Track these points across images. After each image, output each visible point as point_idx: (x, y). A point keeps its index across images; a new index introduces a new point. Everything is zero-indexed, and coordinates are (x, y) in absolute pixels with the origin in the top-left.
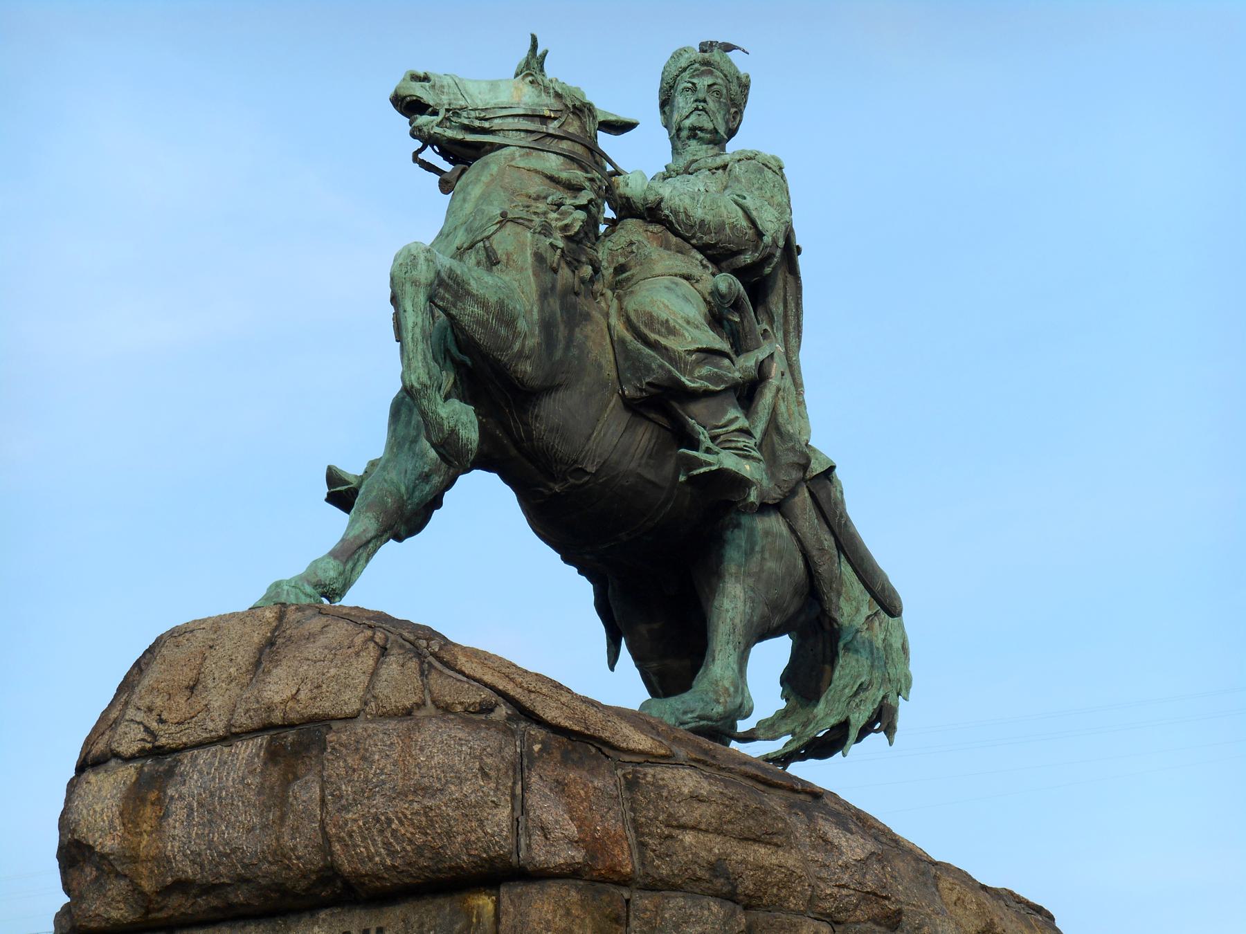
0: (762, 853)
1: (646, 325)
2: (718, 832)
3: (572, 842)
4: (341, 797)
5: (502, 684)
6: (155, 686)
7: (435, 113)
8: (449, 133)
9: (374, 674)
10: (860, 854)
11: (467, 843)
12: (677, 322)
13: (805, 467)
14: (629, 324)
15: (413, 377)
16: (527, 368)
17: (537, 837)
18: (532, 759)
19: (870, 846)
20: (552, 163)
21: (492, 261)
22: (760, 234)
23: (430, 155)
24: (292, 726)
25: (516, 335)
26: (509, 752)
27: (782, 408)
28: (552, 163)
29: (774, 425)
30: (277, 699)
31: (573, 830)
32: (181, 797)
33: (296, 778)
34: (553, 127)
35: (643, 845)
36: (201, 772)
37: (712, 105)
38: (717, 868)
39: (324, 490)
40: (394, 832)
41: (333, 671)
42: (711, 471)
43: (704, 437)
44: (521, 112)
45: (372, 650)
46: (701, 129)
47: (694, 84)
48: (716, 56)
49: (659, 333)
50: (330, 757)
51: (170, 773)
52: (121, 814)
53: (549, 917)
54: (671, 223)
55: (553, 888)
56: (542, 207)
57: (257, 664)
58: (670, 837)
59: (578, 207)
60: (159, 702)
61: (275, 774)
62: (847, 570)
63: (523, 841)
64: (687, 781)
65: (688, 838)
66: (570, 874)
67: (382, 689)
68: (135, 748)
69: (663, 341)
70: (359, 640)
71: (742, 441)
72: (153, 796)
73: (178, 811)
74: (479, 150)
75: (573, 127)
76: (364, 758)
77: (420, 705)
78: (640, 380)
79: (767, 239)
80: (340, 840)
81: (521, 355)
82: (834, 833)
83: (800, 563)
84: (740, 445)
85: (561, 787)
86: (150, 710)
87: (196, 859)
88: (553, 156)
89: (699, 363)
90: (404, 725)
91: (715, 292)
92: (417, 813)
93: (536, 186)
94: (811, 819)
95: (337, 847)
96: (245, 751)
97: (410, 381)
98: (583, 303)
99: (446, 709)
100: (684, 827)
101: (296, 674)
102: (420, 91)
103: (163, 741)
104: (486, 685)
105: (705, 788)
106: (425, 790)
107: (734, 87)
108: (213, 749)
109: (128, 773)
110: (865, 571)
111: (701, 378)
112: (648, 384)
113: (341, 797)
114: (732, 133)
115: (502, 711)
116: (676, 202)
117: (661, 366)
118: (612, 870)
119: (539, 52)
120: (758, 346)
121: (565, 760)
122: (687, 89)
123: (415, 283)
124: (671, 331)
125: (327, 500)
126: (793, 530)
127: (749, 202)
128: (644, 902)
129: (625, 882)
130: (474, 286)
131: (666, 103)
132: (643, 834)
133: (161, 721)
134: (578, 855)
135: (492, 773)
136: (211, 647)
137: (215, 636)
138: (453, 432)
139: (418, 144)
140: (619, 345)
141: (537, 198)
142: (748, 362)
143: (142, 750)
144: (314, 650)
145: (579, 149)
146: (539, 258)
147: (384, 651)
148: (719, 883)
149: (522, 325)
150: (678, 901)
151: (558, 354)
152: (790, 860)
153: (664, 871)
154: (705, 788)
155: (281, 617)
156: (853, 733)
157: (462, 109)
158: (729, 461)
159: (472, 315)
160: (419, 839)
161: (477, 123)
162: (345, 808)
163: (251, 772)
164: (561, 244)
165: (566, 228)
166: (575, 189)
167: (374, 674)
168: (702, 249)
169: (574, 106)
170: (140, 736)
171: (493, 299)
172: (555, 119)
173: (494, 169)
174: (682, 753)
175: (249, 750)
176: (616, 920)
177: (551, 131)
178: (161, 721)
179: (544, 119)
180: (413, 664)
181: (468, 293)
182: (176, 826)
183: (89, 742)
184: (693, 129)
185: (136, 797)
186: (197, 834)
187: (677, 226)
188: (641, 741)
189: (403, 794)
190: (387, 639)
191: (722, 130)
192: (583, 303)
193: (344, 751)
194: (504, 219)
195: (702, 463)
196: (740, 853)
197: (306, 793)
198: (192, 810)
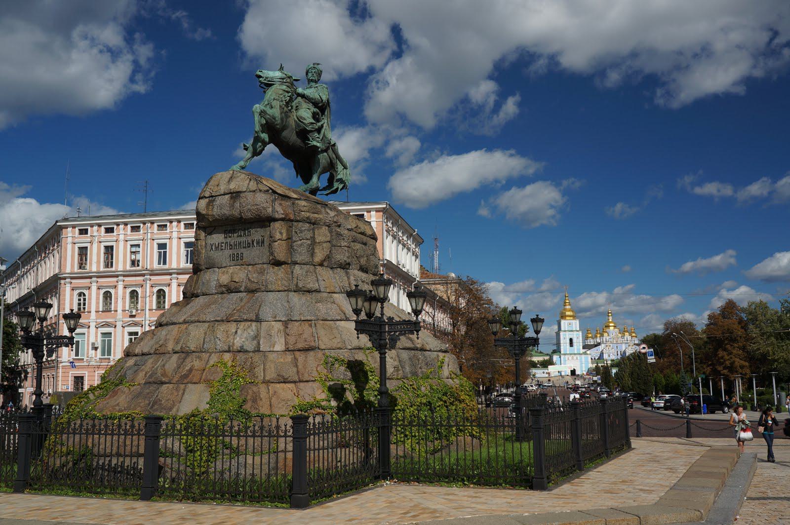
0: (316, 215)
3: (283, 214)
8: (266, 82)
9: (249, 184)
10: (333, 215)
12: (306, 118)
13: (330, 143)
14: (297, 117)
16: (278, 126)
17: (276, 213)
18: (276, 199)
19: (336, 213)
20: (284, 87)
21: (272, 107)
22: (322, 100)
24: (234, 193)
25: (276, 121)
26: (271, 198)
27: (326, 133)
28: (284, 87)
29: (324, 135)
31: (282, 212)
34: (285, 81)
35: (295, 214)
37: (315, 75)
38: (308, 218)
43: (311, 139)
45: (249, 180)
48: (316, 66)
51: (214, 200)
56: (282, 96)
57: (229, 181)
59: (288, 96)
60: (212, 188)
61: (232, 201)
62: (338, 162)
64: (303, 203)
65: (303, 213)
66: (282, 219)
67: (250, 187)
70: (246, 178)
71: (318, 139)
72: (211, 204)
74: (270, 85)
75: (289, 80)
79: (324, 101)
81: (277, 125)
82: (329, 211)
83: (329, 160)
85: (281, 204)
87: (219, 215)
89: (310, 125)
91: (314, 112)
93: (281, 92)
94: (325, 209)
95: (242, 214)
98: (289, 114)
99: (261, 191)
100: (301, 211)
102: (260, 73)
105: (306, 204)
106: (257, 205)
107: (319, 72)
109: (207, 200)
114: (319, 80)
115: (271, 191)
116: (307, 94)
120: (321, 121)
121: (282, 200)
123: (257, 112)
124: (305, 119)
126: (328, 154)
128: (295, 224)
129: (292, 221)
130: (268, 112)
131: (307, 74)
134: (283, 216)
138: (264, 139)
139: (260, 84)
140: (295, 121)
141: (281, 94)
142: (319, 124)
144: (238, 179)
145: (289, 85)
146: (280, 106)
147: (250, 180)
148: (308, 221)
149: (277, 119)
150: (301, 223)
151: (284, 124)
152: (321, 216)
153: (299, 219)
154: (306, 204)
155: (233, 173)
156: (339, 190)
158: (315, 143)
160: (256, 213)
162: (244, 207)
164: (285, 103)
165: (286, 100)
166: (288, 92)
167: (249, 184)
168: (312, 103)
171: (271, 115)
173: (273, 89)
174: (302, 198)
176: (290, 227)
179: (283, 79)
180: (255, 182)
182: (215, 210)
183: (201, 194)
184: (312, 80)
185: (208, 205)
188: (295, 196)
189: (253, 205)
191: (317, 80)
192: (289, 114)
194: (274, 99)
196: (312, 215)
197: (237, 205)
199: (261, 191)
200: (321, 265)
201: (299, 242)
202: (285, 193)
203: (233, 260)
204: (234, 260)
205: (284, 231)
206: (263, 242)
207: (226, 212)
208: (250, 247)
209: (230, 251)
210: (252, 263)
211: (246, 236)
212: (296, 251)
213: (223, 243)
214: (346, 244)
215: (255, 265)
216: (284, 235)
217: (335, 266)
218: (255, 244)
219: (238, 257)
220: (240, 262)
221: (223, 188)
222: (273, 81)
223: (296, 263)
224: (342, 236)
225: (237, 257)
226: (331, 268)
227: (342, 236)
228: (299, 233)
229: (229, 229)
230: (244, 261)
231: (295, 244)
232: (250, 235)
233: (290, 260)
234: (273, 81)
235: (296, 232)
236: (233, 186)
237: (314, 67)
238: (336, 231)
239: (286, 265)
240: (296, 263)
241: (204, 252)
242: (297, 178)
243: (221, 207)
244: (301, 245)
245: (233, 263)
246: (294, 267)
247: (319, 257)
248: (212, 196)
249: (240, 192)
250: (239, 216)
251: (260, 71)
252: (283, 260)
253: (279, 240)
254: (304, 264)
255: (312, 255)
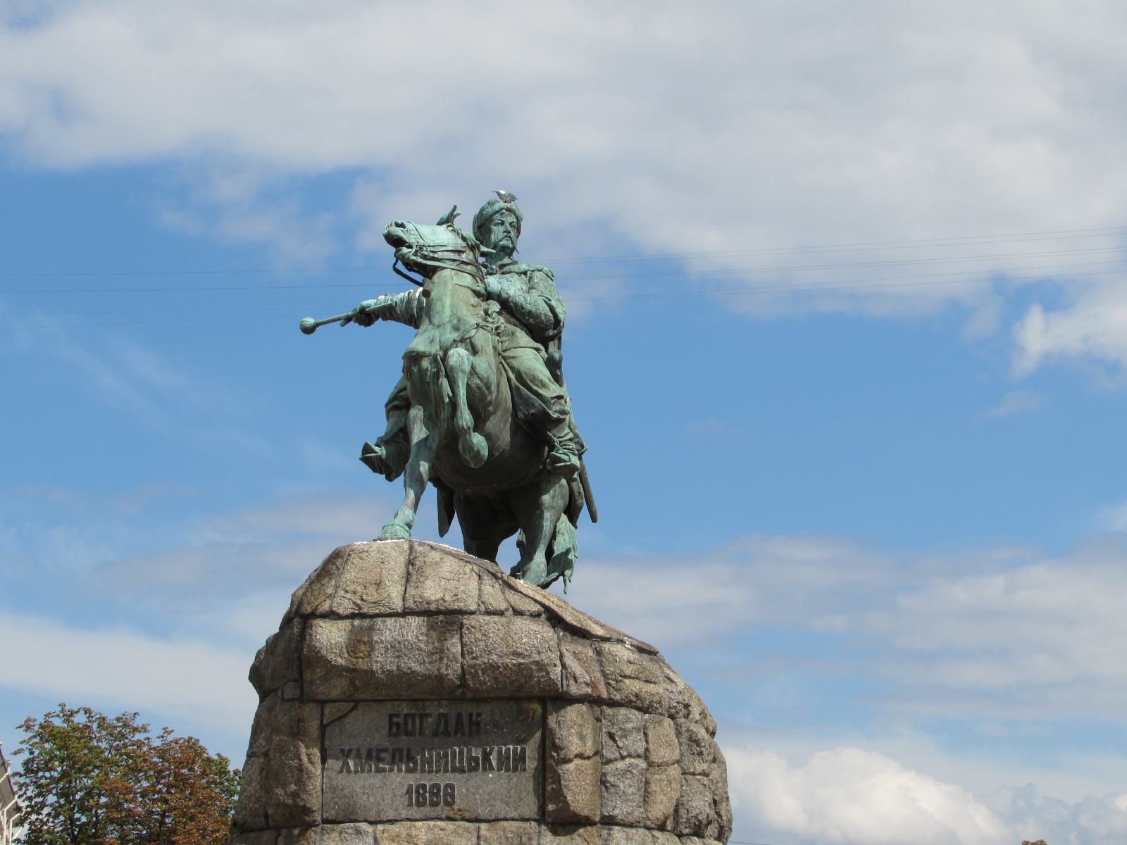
1: (531, 381)
2: (637, 678)
3: (587, 684)
4: (472, 653)
5: (547, 603)
6: (355, 580)
7: (410, 247)
9: (480, 590)
11: (539, 682)
15: (464, 424)
17: (572, 682)
23: (400, 266)
24: (438, 612)
25: (490, 393)
30: (433, 598)
32: (382, 642)
33: (446, 640)
35: (609, 684)
36: (390, 630)
39: (359, 454)
40: (501, 673)
41: (462, 588)
42: (566, 465)
44: (450, 249)
46: (508, 248)
47: (503, 221)
49: (537, 386)
50: (467, 632)
51: (371, 628)
52: (347, 647)
53: (575, 719)
54: (512, 310)
55: (576, 706)
58: (621, 681)
63: (564, 682)
65: (627, 681)
68: (348, 612)
69: (541, 391)
73: (380, 648)
76: (484, 635)
77: (507, 610)
78: (528, 411)
80: (471, 673)
84: (570, 447)
86: (354, 593)
88: (468, 275)
90: (503, 619)
92: (514, 665)
96: (415, 622)
97: (463, 425)
99: (518, 613)
100: (625, 677)
101: (439, 586)
102: (399, 232)
103: (365, 610)
104: (536, 601)
108: (393, 619)
110: (591, 501)
111: (556, 412)
112: (532, 414)
113: (472, 653)
117: (540, 405)
118: (599, 697)
119: (455, 213)
122: (499, 224)
123: (463, 372)
124: (544, 386)
125: (361, 459)
127: (554, 303)
128: (609, 711)
132: (609, 679)
133: (362, 600)
134: (589, 690)
135: (553, 649)
136: (383, 563)
137: (383, 557)
138: (478, 452)
143: (353, 613)
146: (495, 348)
150: (623, 711)
153: (618, 697)
157: (423, 246)
159: (476, 384)
161: (432, 255)
163: (421, 634)
169: (472, 245)
170: (350, 606)
171: (486, 376)
172: (463, 252)
175: (417, 622)
177: (464, 260)
178: (362, 600)
179: (459, 252)
181: (476, 373)
186: (390, 661)
187: (515, 311)
190: (480, 570)
193: (473, 630)
195: (561, 460)
198: (388, 649)
199: (518, 613)
200: (662, 828)
201: (620, 765)
202: (580, 621)
203: (419, 804)
204: (424, 804)
205: (588, 732)
206: (521, 758)
207: (416, 667)
208: (476, 769)
209: (411, 776)
210: (483, 812)
211: (463, 734)
212: (613, 790)
213: (385, 750)
214: (705, 766)
215: (497, 820)
216: (589, 743)
217: (687, 831)
218: (494, 763)
219: (437, 795)
220: (442, 810)
221: (394, 595)
222: (433, 259)
223: (609, 821)
224: (698, 745)
225: (432, 794)
226: (680, 836)
227: (698, 745)
228: (621, 737)
229: (405, 712)
230: (456, 807)
231: (609, 768)
232: (478, 733)
233: (598, 812)
234: (433, 259)
235: (611, 736)
236: (432, 591)
237: (509, 210)
238: (688, 730)
239: (589, 828)
240: (609, 821)
241: (319, 772)
242: (443, 529)
243: (397, 648)
244: (628, 771)
245: (415, 812)
246: (609, 835)
247: (661, 807)
248: (362, 616)
249: (462, 612)
250: (437, 672)
251: (398, 225)
252: (585, 812)
253: (576, 756)
254: (631, 825)
255: (646, 796)
